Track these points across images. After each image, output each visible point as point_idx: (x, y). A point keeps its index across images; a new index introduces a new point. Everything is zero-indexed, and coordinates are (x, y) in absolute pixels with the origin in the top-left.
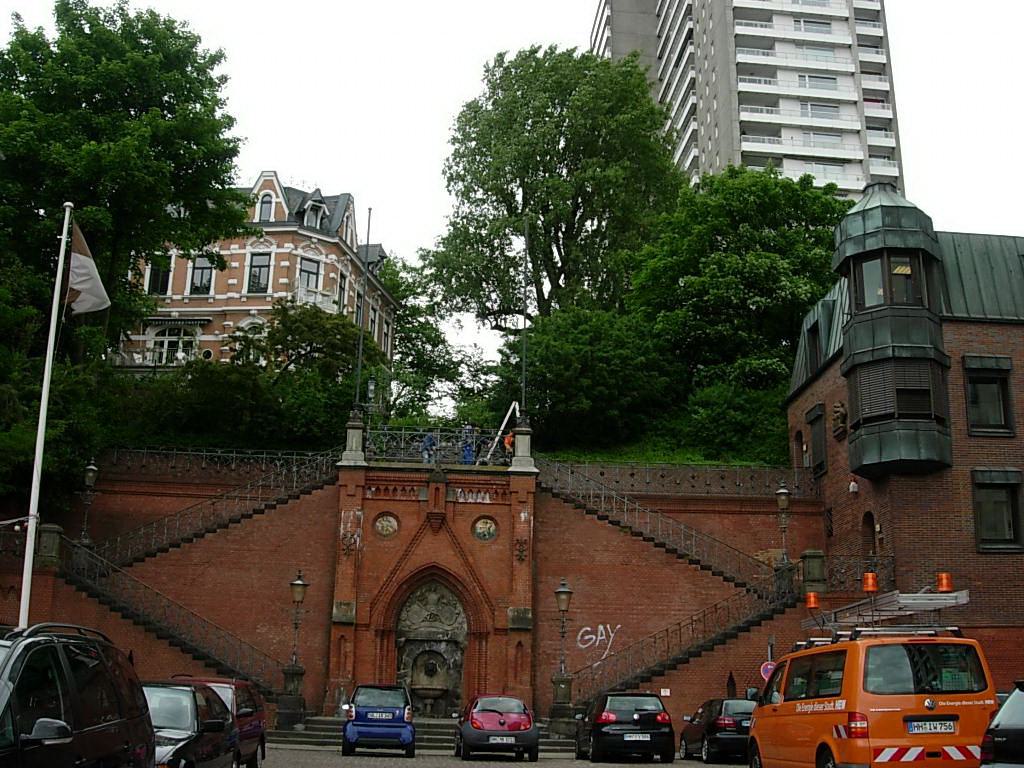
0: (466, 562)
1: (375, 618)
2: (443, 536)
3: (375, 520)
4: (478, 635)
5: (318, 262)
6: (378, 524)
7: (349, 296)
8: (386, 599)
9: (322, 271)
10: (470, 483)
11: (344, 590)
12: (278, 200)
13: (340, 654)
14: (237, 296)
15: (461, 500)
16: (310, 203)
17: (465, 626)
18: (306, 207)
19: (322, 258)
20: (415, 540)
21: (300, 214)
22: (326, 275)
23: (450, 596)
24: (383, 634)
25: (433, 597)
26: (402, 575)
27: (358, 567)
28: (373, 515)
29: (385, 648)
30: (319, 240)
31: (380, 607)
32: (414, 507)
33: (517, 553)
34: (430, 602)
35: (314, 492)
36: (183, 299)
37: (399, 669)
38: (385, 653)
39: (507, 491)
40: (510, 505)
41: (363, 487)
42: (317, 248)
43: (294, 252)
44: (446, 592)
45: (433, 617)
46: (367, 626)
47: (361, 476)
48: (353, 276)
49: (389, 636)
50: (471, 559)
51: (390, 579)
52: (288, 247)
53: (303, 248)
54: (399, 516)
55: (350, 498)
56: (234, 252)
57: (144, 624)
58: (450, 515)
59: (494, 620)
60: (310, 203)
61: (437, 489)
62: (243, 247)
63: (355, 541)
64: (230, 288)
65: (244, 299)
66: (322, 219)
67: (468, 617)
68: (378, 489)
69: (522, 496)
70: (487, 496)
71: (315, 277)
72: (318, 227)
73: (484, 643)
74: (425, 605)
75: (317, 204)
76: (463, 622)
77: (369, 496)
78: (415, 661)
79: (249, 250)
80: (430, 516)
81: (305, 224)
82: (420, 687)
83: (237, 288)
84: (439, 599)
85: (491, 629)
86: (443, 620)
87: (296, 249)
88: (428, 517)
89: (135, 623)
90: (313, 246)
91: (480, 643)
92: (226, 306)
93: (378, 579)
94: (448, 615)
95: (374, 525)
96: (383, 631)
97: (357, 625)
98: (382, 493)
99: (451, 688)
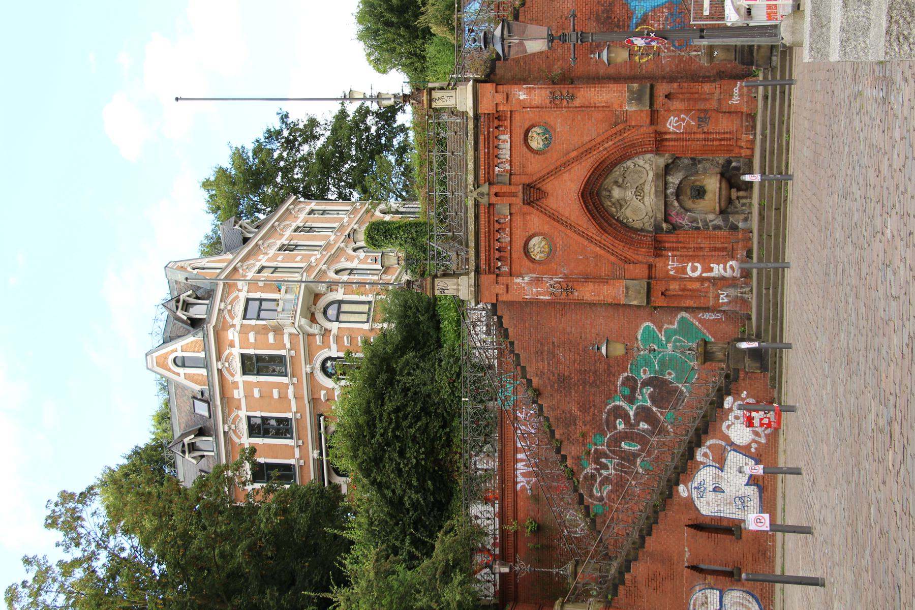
0: (577, 159)
1: (641, 259)
2: (548, 186)
3: (532, 261)
4: (659, 143)
5: (248, 300)
6: (537, 258)
7: (282, 261)
8: (620, 247)
9: (257, 295)
11: (613, 291)
12: (179, 349)
13: (681, 296)
14: (291, 390)
15: (507, 167)
16: (180, 313)
17: (648, 156)
18: (185, 318)
19: (243, 296)
20: (555, 217)
21: (195, 323)
22: (262, 290)
24: (658, 249)
25: (616, 193)
26: (592, 230)
27: (587, 278)
28: (529, 264)
29: (674, 245)
30: (221, 301)
31: (629, 254)
32: (518, 220)
34: (622, 195)
35: (505, 326)
36: (299, 446)
37: (699, 228)
38: (681, 245)
40: (511, 112)
41: (498, 275)
42: (232, 303)
43: (238, 327)
44: (610, 179)
45: (639, 192)
46: (650, 267)
47: (486, 279)
48: (261, 257)
49: (660, 242)
51: (598, 244)
52: (232, 335)
53: (233, 318)
55: (511, 289)
56: (242, 394)
57: (656, 512)
60: (180, 313)
61: (496, 194)
62: (236, 384)
63: (558, 282)
64: (283, 397)
65: (295, 380)
66: (197, 298)
67: (637, 154)
68: (498, 259)
69: (500, 98)
70: (503, 137)
71: (264, 303)
72: (207, 302)
73: (668, 136)
75: (180, 305)
77: (505, 269)
78: (687, 210)
79: (239, 378)
80: (529, 202)
81: (204, 317)
82: (717, 205)
83: (283, 388)
84: (619, 186)
85: (651, 129)
86: (641, 181)
87: (233, 326)
88: (529, 204)
89: (656, 522)
90: (229, 307)
91: (666, 140)
92: (303, 398)
93: (597, 256)
95: (539, 263)
96: (655, 248)
97: (650, 277)
98: (502, 254)
99: (718, 170)
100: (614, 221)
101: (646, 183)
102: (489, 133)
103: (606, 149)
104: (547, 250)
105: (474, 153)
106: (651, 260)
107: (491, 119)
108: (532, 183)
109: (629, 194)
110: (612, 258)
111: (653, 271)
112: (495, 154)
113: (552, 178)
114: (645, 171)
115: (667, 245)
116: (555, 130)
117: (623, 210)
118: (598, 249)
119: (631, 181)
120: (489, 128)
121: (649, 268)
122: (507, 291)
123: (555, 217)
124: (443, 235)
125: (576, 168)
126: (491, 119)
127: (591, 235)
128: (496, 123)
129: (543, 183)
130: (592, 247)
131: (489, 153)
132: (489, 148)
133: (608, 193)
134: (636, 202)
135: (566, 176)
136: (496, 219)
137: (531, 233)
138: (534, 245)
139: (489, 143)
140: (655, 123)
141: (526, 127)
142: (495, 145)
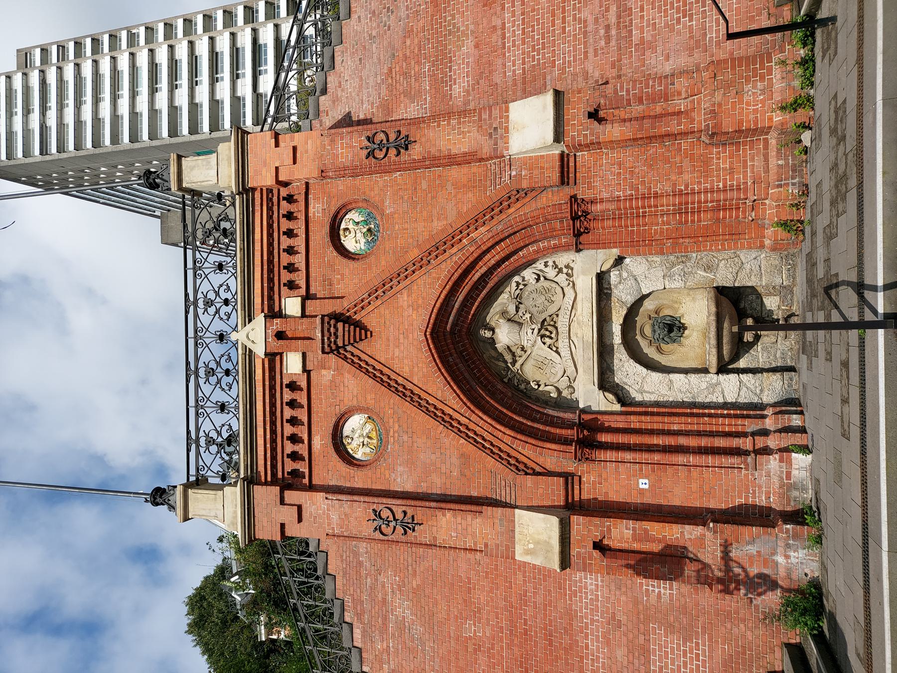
0: (420, 264)
3: (347, 458)
6: (359, 456)
8: (505, 438)
10: (271, 271)
17: (563, 259)
23: (504, 300)
27: (445, 500)
29: (621, 439)
33: (392, 152)
39: (284, 192)
44: (496, 308)
50: (414, 254)
51: (463, 432)
54: (338, 410)
58: (330, 307)
59: (545, 188)
73: (597, 208)
74: (523, 349)
76: (555, 266)
80: (333, 349)
86: (552, 309)
94: (541, 300)
98: (297, 448)
100: (500, 386)
101: (561, 313)
103: (473, 240)
104: (375, 441)
106: (570, 466)
108: (342, 314)
109: (528, 336)
110: (490, 462)
111: (577, 492)
113: (379, 302)
114: (559, 290)
115: (604, 438)
116: (382, 213)
117: (518, 365)
118: (462, 441)
119: (534, 310)
121: (566, 484)
122: (300, 520)
123: (385, 378)
125: (420, 282)
126: (275, 199)
127: (451, 412)
129: (363, 313)
130: (451, 442)
133: (488, 334)
134: (541, 350)
135: (404, 299)
136: (285, 382)
137: (343, 410)
140: (572, 181)
141: (333, 209)
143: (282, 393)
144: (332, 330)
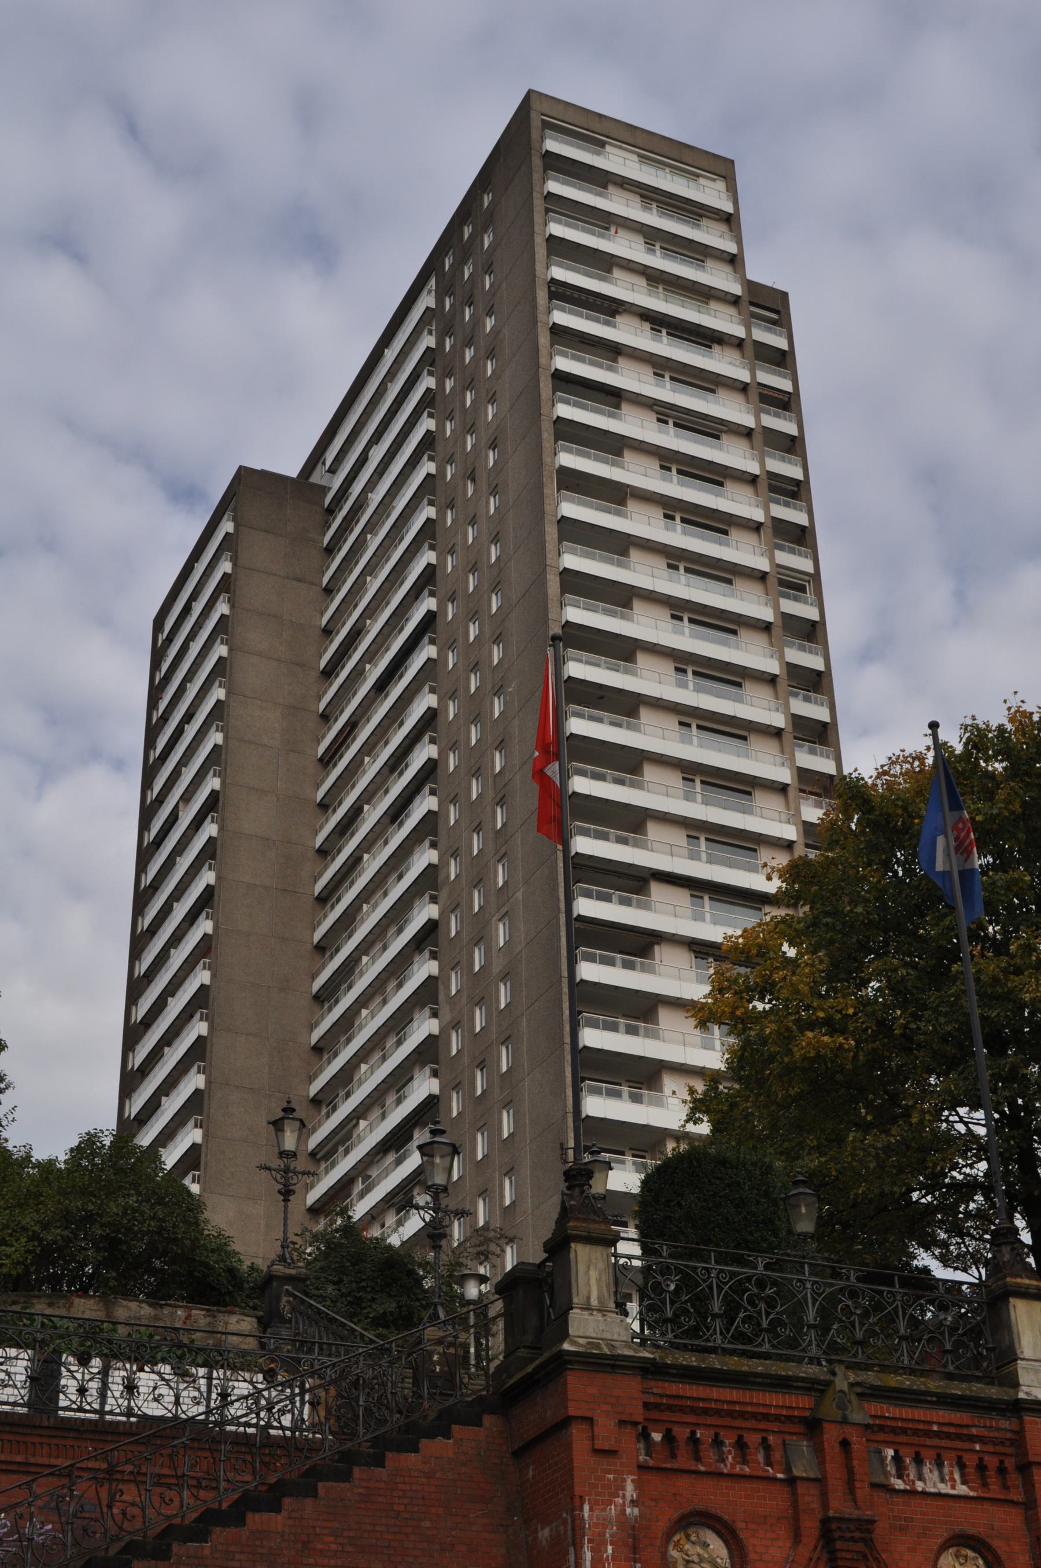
10: (916, 1432)
68: (669, 1438)
102: (972, 1439)
105: (932, 1394)
107: (1000, 1449)
112: (924, 1452)
120: (980, 1439)
124: (710, 1287)
126: (1000, 1449)
128: (992, 1462)
131: (928, 1434)
132: (938, 1435)
138: (705, 1545)
139: (948, 1436)
141: (995, 1544)
142: (944, 1454)
143: (755, 1430)
144: (857, 1535)
